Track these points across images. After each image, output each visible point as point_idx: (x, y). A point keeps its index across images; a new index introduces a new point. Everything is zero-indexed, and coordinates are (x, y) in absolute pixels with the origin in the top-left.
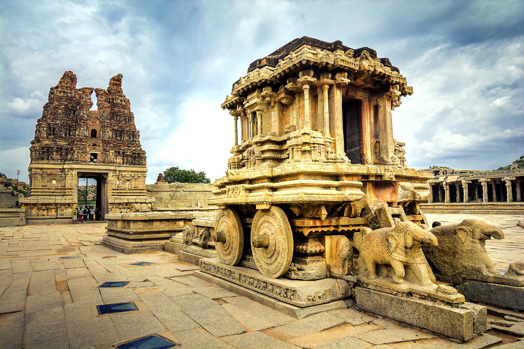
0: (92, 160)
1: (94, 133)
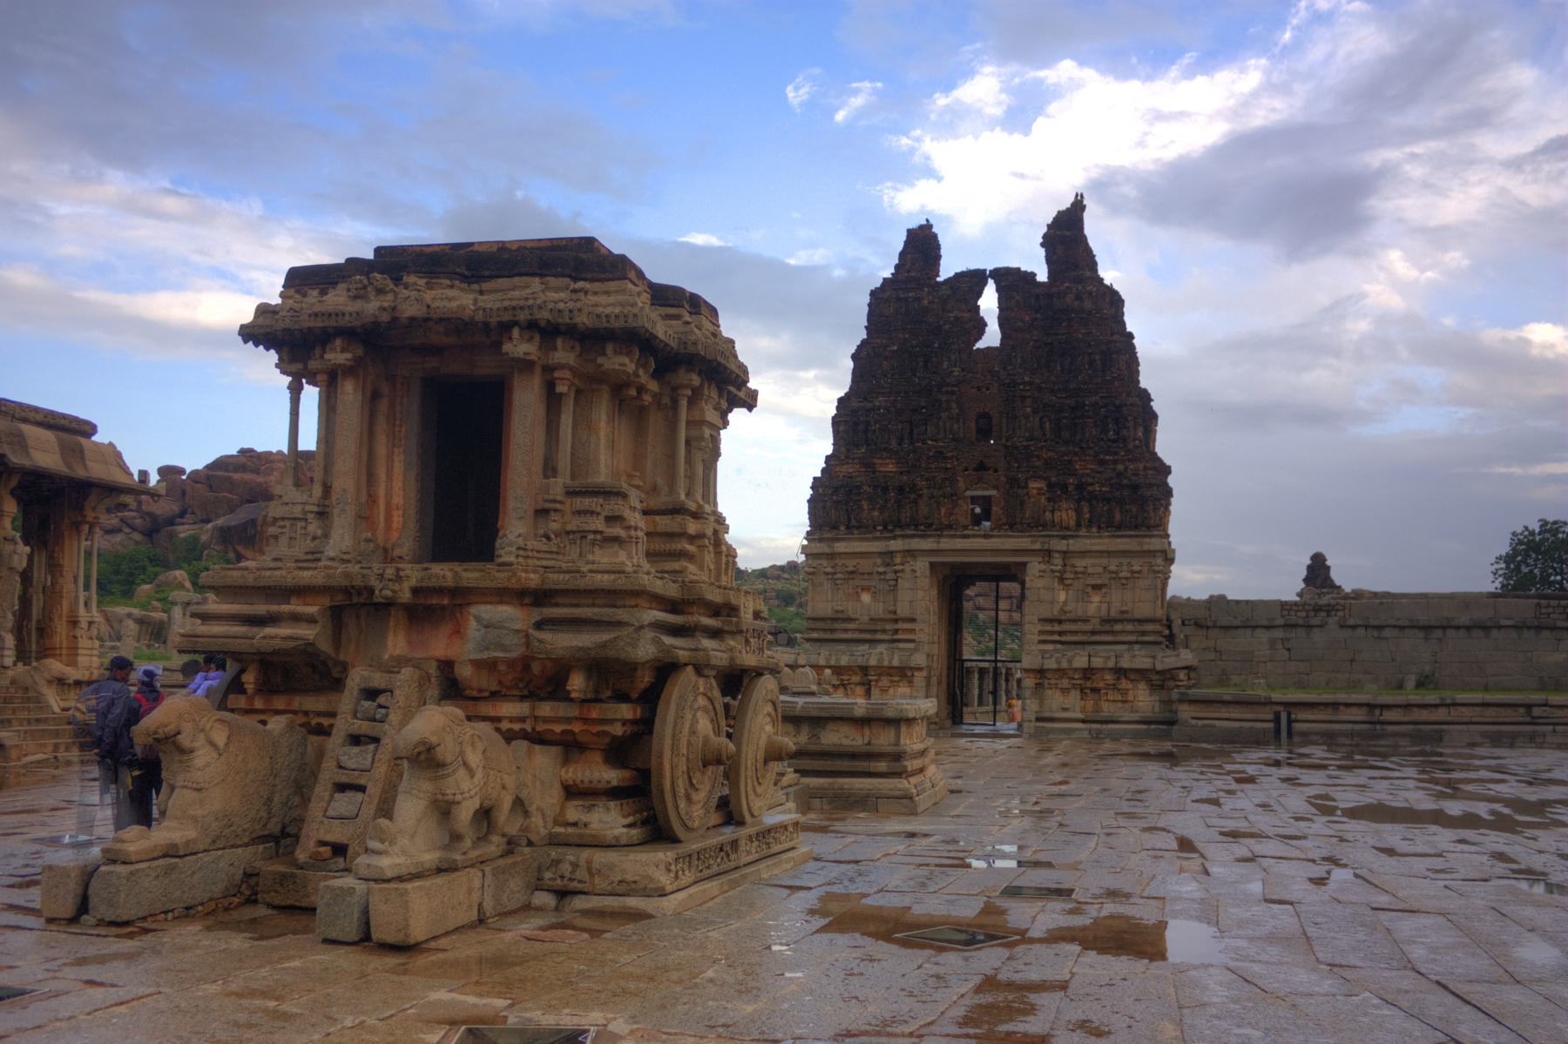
0: (977, 520)
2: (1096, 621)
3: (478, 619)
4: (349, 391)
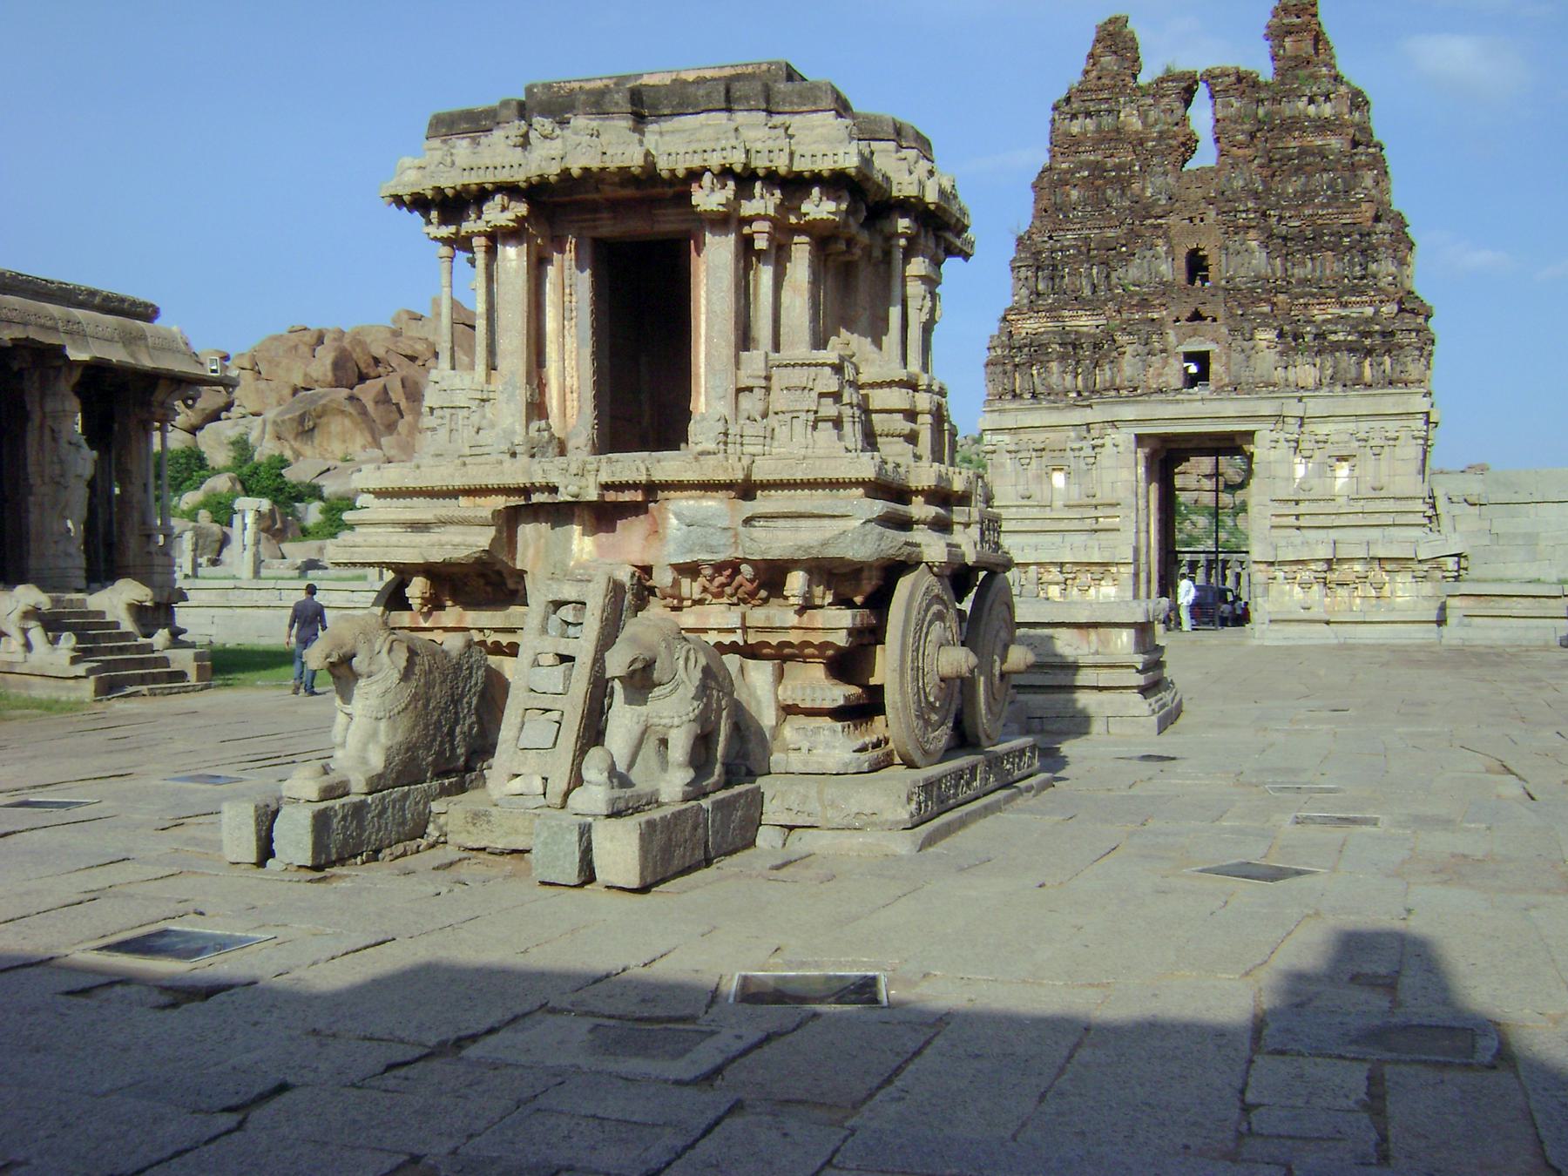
0: (1191, 381)
1: (1196, 265)
2: (1341, 501)
3: (678, 516)
4: (513, 256)
